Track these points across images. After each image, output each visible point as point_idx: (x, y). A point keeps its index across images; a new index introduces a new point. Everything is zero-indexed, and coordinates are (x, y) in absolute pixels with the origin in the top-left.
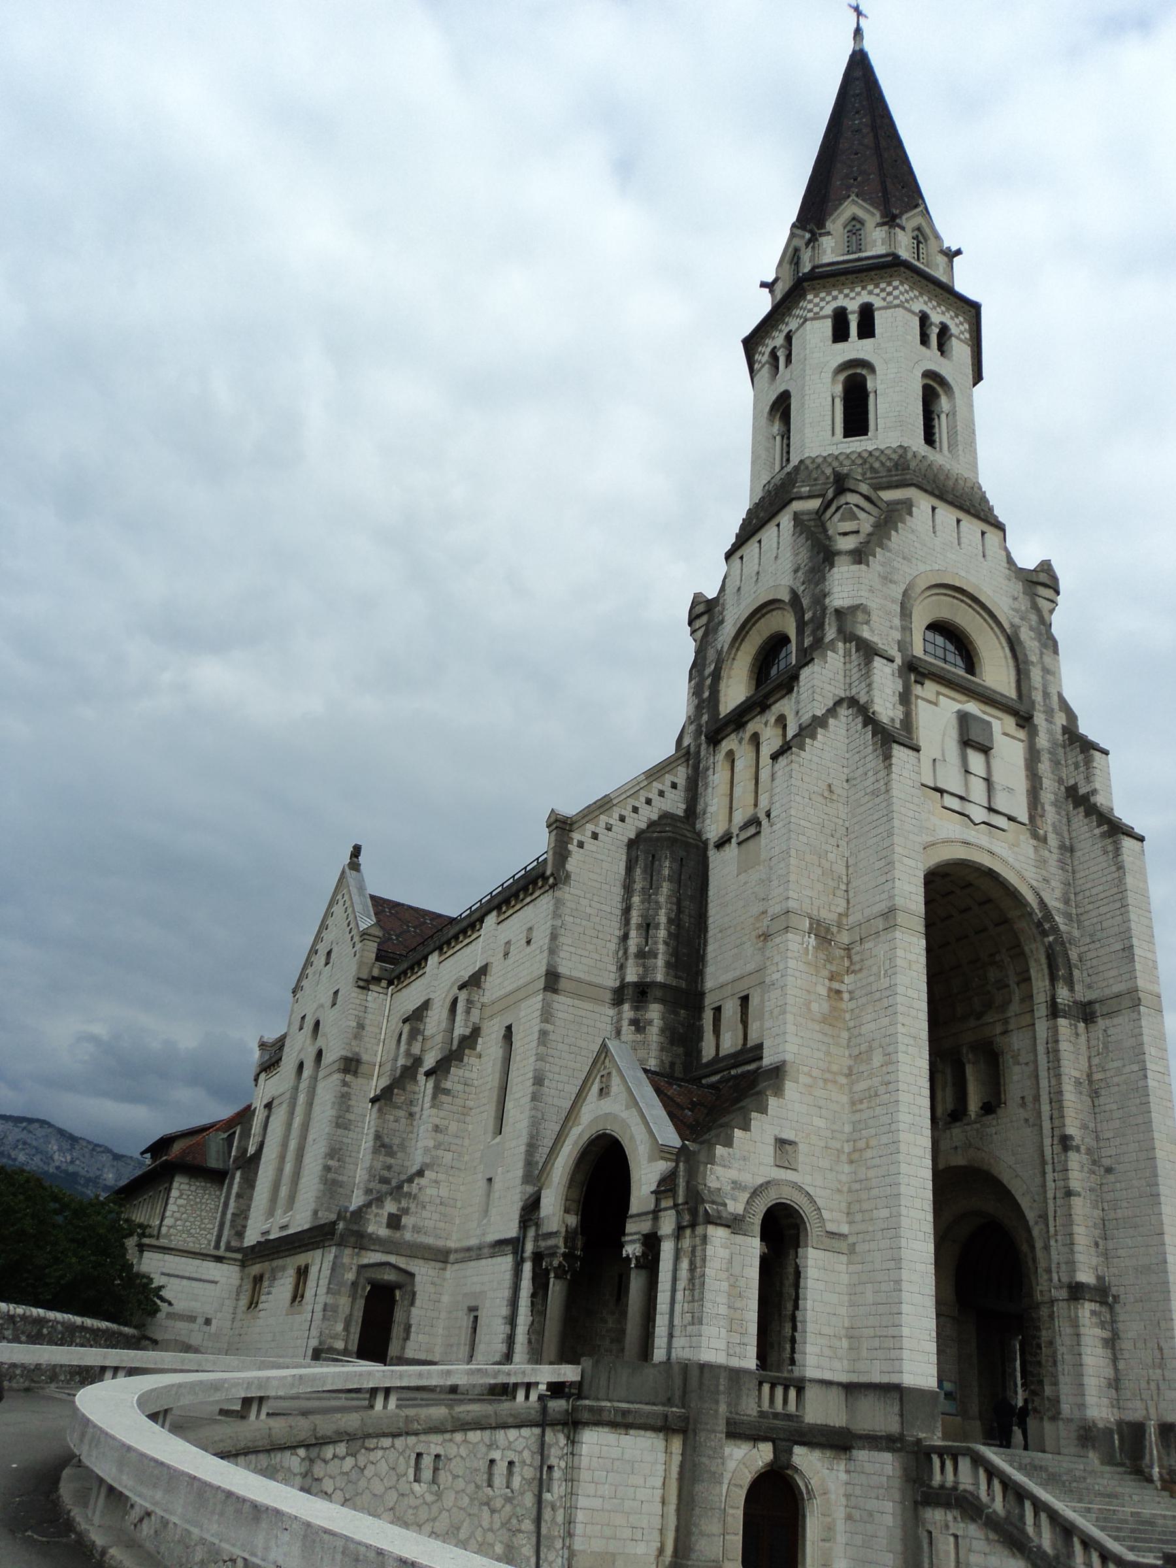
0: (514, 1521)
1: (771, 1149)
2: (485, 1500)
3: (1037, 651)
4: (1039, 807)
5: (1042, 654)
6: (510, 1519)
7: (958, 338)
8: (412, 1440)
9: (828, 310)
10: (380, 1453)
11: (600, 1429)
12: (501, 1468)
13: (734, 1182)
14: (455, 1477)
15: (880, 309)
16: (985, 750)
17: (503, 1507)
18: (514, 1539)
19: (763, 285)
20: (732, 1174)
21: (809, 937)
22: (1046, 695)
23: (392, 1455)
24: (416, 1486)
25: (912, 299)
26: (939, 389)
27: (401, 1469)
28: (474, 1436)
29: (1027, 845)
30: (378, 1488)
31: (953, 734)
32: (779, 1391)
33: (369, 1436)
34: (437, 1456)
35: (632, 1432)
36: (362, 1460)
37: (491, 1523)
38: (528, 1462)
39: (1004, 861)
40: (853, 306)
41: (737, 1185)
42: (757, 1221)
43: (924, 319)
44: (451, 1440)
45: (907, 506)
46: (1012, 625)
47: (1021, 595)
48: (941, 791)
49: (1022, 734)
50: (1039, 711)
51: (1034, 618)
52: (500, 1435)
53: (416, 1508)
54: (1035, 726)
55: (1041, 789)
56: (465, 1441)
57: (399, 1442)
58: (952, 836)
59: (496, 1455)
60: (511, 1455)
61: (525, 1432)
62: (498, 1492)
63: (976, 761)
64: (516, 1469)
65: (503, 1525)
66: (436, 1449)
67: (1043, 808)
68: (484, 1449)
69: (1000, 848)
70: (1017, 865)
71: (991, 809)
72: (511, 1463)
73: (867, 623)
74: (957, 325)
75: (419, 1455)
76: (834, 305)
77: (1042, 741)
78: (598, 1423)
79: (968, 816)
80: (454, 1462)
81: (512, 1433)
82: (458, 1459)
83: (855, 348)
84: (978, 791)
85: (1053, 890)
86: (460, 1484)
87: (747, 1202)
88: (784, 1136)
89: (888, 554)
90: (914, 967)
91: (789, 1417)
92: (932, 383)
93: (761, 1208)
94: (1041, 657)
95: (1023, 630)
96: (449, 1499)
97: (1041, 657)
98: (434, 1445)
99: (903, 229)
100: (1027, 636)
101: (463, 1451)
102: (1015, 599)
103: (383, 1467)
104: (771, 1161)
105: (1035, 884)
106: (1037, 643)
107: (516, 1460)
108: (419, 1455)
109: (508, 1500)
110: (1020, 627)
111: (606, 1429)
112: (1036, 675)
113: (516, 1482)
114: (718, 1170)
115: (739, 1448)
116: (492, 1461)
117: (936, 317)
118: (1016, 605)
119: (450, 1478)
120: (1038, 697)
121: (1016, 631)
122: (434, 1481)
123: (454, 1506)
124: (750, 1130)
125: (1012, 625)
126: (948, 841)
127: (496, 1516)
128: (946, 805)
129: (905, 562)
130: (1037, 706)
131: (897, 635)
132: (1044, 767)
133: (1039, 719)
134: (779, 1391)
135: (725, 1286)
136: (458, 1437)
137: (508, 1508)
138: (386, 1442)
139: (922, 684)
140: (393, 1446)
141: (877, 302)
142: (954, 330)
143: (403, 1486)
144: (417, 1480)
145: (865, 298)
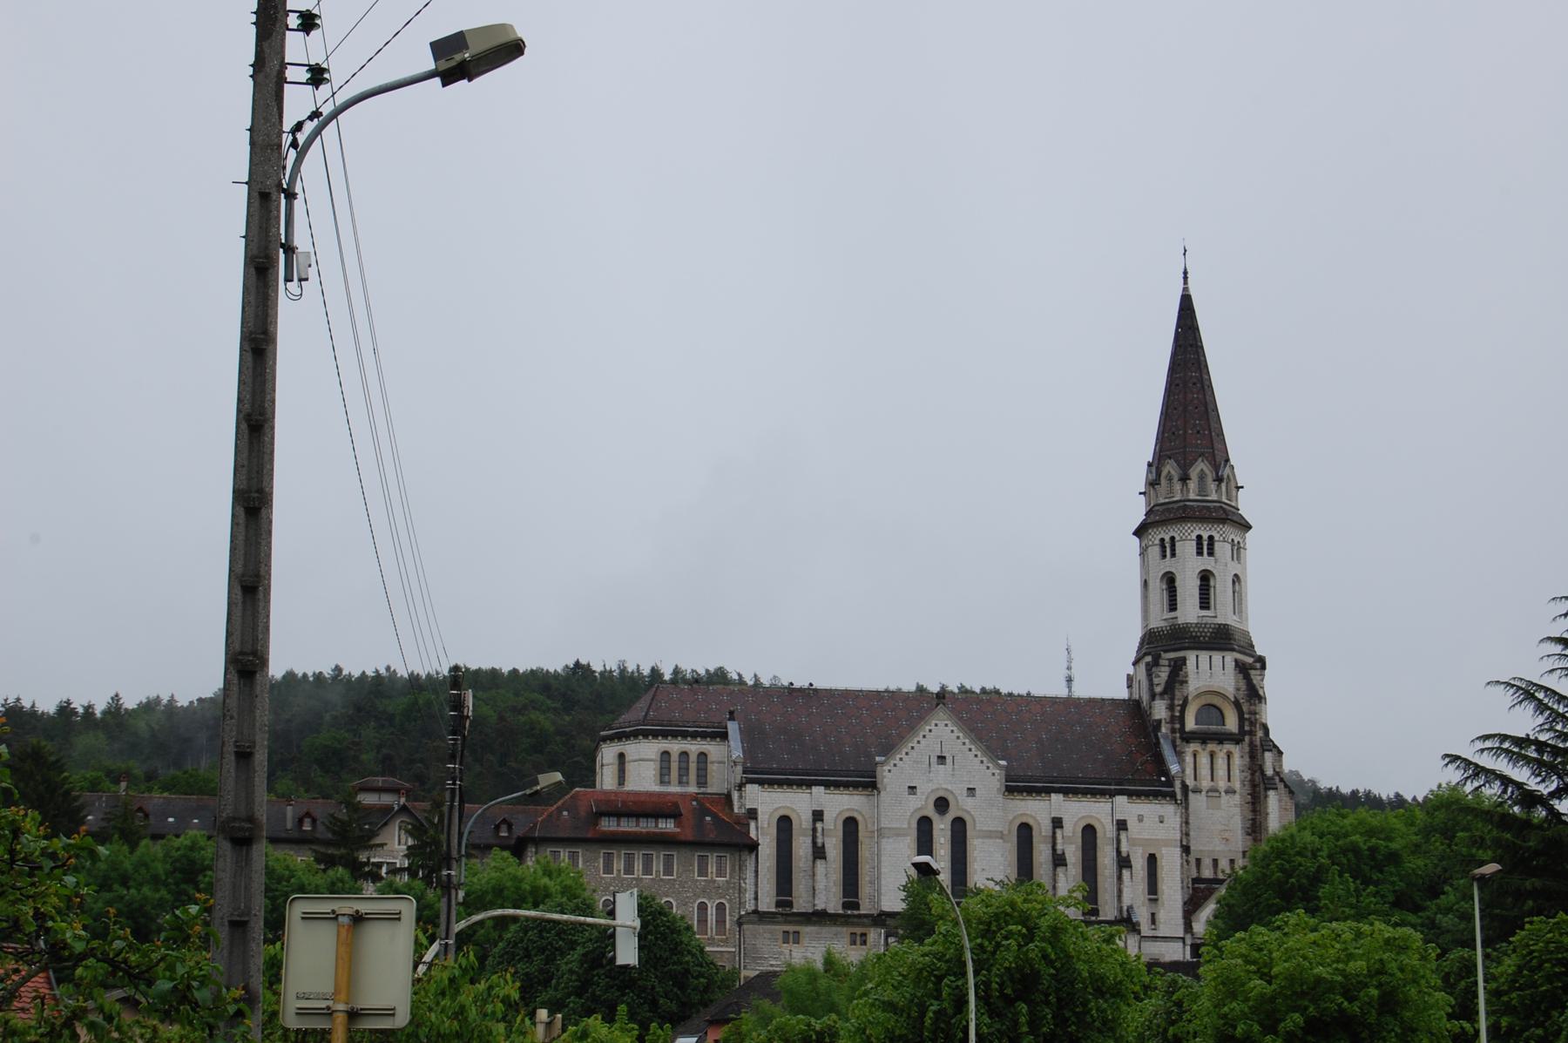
7: (1218, 541)
9: (1157, 542)
15: (1178, 541)
19: (1141, 493)
25: (1192, 531)
26: (1208, 574)
40: (1167, 539)
43: (1199, 537)
45: (1184, 660)
74: (1218, 532)
76: (1160, 537)
83: (1169, 565)
117: (1205, 536)
141: (1177, 538)
142: (1216, 538)
145: (1172, 534)
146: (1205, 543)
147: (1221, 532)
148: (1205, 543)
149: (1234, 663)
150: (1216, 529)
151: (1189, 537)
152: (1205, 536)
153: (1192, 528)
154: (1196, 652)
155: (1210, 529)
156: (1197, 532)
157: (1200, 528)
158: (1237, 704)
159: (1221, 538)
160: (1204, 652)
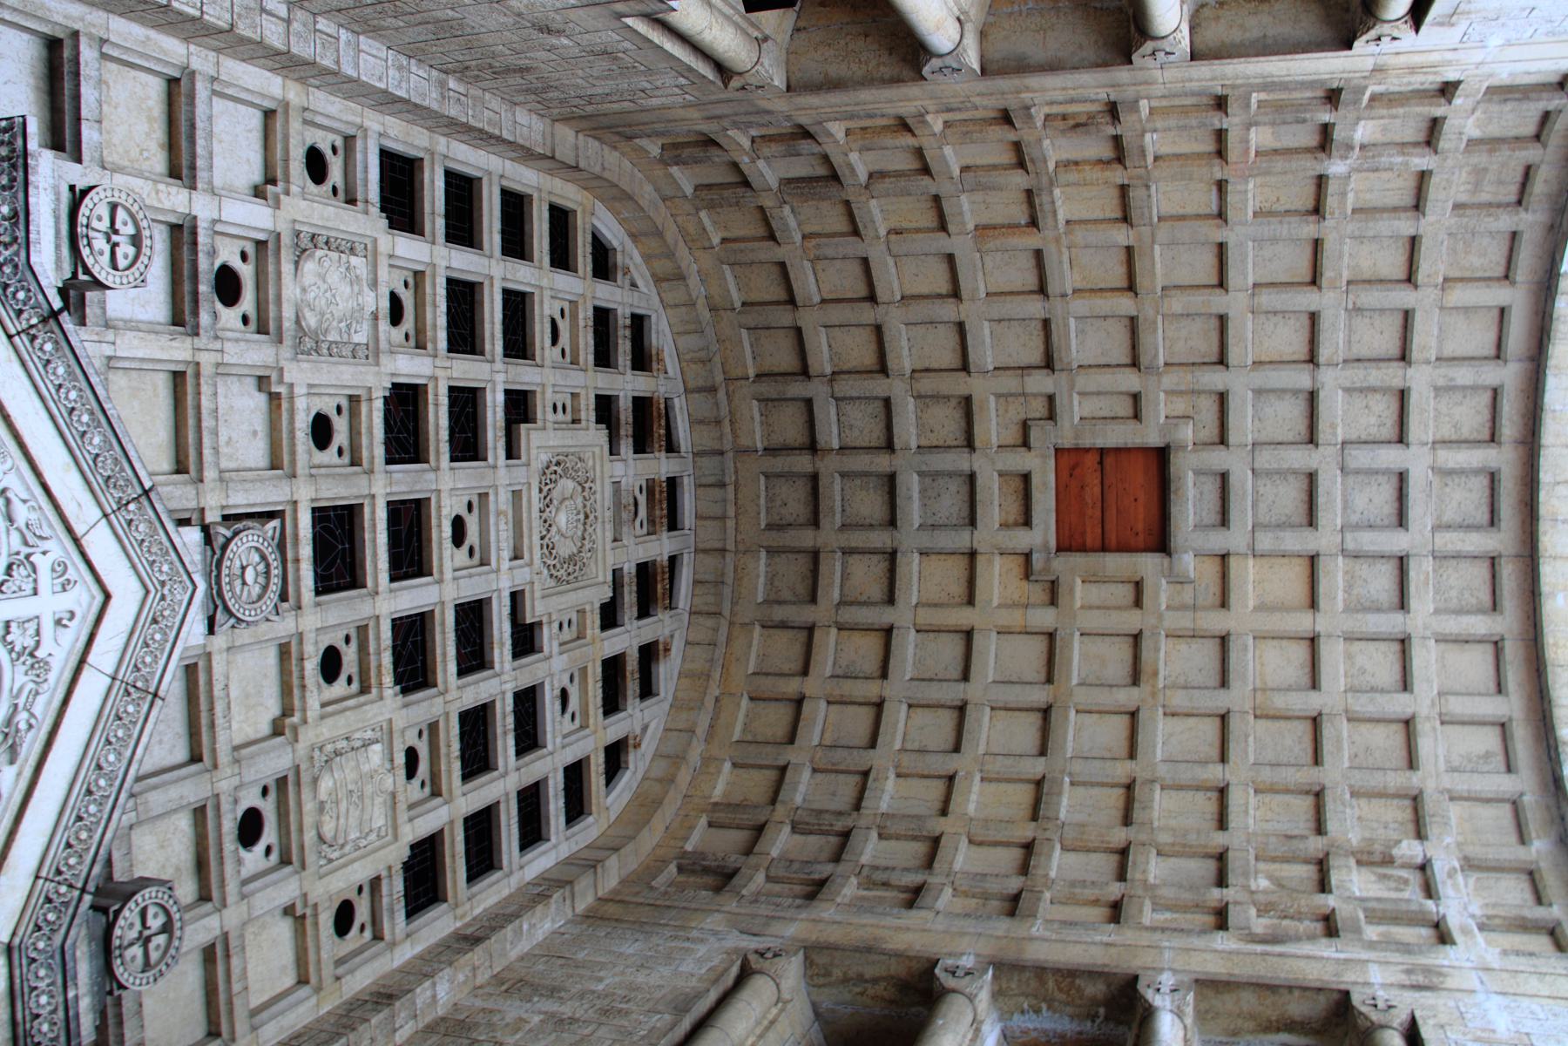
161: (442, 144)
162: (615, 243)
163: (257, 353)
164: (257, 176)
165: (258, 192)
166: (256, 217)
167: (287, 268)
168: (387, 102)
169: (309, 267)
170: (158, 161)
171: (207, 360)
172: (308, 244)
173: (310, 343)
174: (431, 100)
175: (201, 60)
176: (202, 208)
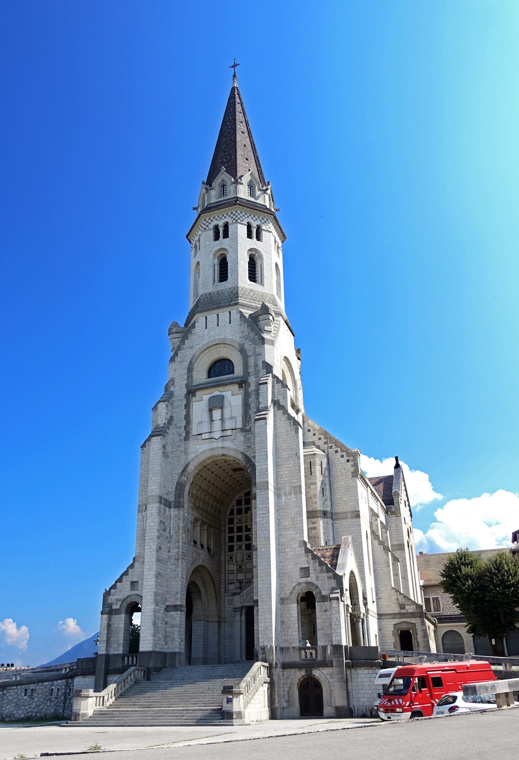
0: (58, 704)
1: (129, 586)
2: (49, 699)
3: (253, 348)
4: (248, 417)
5: (255, 348)
6: (57, 703)
8: (24, 686)
10: (12, 690)
11: (79, 677)
12: (55, 691)
13: (116, 599)
14: (38, 694)
16: (222, 408)
17: (55, 700)
18: (57, 708)
20: (116, 597)
21: (145, 512)
22: (256, 365)
23: (16, 691)
24: (25, 697)
27: (19, 692)
28: (45, 684)
29: (240, 437)
30: (10, 698)
31: (207, 409)
32: (130, 658)
33: (7, 686)
34: (32, 690)
35: (88, 677)
36: (5, 692)
37: (51, 704)
38: (64, 688)
39: (229, 448)
41: (117, 600)
42: (123, 610)
44: (38, 685)
46: (240, 345)
47: (246, 328)
48: (201, 434)
49: (242, 391)
50: (252, 375)
51: (252, 335)
52: (55, 683)
53: (24, 702)
54: (249, 384)
55: (250, 409)
56: (43, 685)
57: (19, 687)
58: (205, 449)
59: (53, 687)
60: (58, 687)
61: (64, 681)
62: (53, 697)
63: (217, 414)
64: (60, 690)
65: (54, 705)
66: (31, 688)
67: (250, 417)
68: (49, 686)
69: (228, 444)
70: (235, 447)
71: (223, 430)
72: (58, 689)
73: (173, 384)
74: (232, 218)
75: (26, 690)
77: (252, 388)
78: (78, 675)
79: (213, 438)
80: (38, 690)
81: (59, 682)
82: (40, 689)
84: (217, 425)
85: (252, 449)
86: (40, 696)
87: (121, 605)
88: (134, 580)
89: (183, 351)
90: (153, 515)
91: (314, 660)
92: (222, 252)
93: (125, 605)
94: (255, 350)
95: (246, 344)
96: (36, 699)
97: (255, 350)
98: (32, 686)
99: (213, 189)
100: (248, 346)
101: (41, 687)
102: (243, 332)
103: (13, 693)
104: (129, 589)
105: (242, 451)
106: (253, 346)
107: (60, 688)
108: (26, 690)
109: (56, 698)
110: (244, 344)
111: (81, 677)
112: (251, 361)
113: (60, 693)
114: (112, 597)
115: (116, 677)
116: (52, 689)
118: (244, 334)
119: (37, 694)
120: (251, 370)
121: (243, 347)
122: (32, 695)
123: (38, 701)
124: (122, 582)
125: (240, 345)
126: (204, 452)
127: (52, 703)
128: (203, 438)
129: (191, 349)
130: (251, 374)
131: (185, 382)
132: (252, 400)
133: (252, 380)
134: (130, 658)
135: (106, 632)
136: (40, 684)
137: (56, 700)
138: (15, 687)
139: (195, 396)
140: (17, 688)
142: (230, 222)
143: (20, 697)
144: (25, 695)
146: (221, 230)
147: (234, 217)
148: (221, 230)
149: (239, 315)
150: (229, 216)
151: (207, 228)
152: (221, 223)
153: (210, 221)
154: (205, 314)
155: (225, 217)
156: (215, 223)
157: (216, 220)
158: (242, 351)
159: (234, 221)
160: (211, 312)
161: (227, 543)
162: (230, 509)
163: (244, 565)
164: (232, 565)
165: (234, 565)
166: (235, 566)
167: (238, 563)
168: (225, 554)
169: (238, 560)
170: (233, 574)
171: (245, 571)
172: (237, 561)
173: (243, 561)
174: (224, 550)
175: (227, 572)
176: (235, 572)
